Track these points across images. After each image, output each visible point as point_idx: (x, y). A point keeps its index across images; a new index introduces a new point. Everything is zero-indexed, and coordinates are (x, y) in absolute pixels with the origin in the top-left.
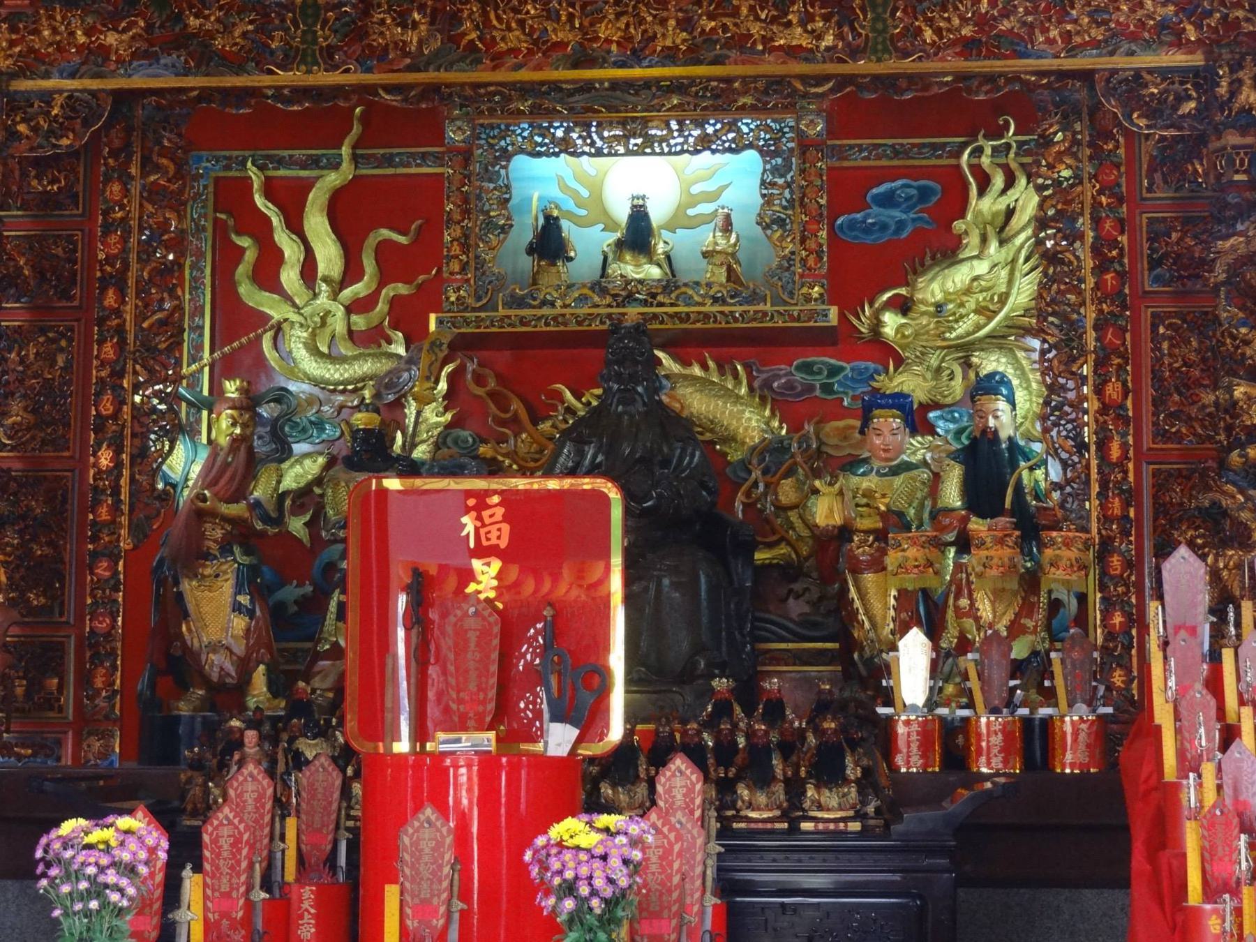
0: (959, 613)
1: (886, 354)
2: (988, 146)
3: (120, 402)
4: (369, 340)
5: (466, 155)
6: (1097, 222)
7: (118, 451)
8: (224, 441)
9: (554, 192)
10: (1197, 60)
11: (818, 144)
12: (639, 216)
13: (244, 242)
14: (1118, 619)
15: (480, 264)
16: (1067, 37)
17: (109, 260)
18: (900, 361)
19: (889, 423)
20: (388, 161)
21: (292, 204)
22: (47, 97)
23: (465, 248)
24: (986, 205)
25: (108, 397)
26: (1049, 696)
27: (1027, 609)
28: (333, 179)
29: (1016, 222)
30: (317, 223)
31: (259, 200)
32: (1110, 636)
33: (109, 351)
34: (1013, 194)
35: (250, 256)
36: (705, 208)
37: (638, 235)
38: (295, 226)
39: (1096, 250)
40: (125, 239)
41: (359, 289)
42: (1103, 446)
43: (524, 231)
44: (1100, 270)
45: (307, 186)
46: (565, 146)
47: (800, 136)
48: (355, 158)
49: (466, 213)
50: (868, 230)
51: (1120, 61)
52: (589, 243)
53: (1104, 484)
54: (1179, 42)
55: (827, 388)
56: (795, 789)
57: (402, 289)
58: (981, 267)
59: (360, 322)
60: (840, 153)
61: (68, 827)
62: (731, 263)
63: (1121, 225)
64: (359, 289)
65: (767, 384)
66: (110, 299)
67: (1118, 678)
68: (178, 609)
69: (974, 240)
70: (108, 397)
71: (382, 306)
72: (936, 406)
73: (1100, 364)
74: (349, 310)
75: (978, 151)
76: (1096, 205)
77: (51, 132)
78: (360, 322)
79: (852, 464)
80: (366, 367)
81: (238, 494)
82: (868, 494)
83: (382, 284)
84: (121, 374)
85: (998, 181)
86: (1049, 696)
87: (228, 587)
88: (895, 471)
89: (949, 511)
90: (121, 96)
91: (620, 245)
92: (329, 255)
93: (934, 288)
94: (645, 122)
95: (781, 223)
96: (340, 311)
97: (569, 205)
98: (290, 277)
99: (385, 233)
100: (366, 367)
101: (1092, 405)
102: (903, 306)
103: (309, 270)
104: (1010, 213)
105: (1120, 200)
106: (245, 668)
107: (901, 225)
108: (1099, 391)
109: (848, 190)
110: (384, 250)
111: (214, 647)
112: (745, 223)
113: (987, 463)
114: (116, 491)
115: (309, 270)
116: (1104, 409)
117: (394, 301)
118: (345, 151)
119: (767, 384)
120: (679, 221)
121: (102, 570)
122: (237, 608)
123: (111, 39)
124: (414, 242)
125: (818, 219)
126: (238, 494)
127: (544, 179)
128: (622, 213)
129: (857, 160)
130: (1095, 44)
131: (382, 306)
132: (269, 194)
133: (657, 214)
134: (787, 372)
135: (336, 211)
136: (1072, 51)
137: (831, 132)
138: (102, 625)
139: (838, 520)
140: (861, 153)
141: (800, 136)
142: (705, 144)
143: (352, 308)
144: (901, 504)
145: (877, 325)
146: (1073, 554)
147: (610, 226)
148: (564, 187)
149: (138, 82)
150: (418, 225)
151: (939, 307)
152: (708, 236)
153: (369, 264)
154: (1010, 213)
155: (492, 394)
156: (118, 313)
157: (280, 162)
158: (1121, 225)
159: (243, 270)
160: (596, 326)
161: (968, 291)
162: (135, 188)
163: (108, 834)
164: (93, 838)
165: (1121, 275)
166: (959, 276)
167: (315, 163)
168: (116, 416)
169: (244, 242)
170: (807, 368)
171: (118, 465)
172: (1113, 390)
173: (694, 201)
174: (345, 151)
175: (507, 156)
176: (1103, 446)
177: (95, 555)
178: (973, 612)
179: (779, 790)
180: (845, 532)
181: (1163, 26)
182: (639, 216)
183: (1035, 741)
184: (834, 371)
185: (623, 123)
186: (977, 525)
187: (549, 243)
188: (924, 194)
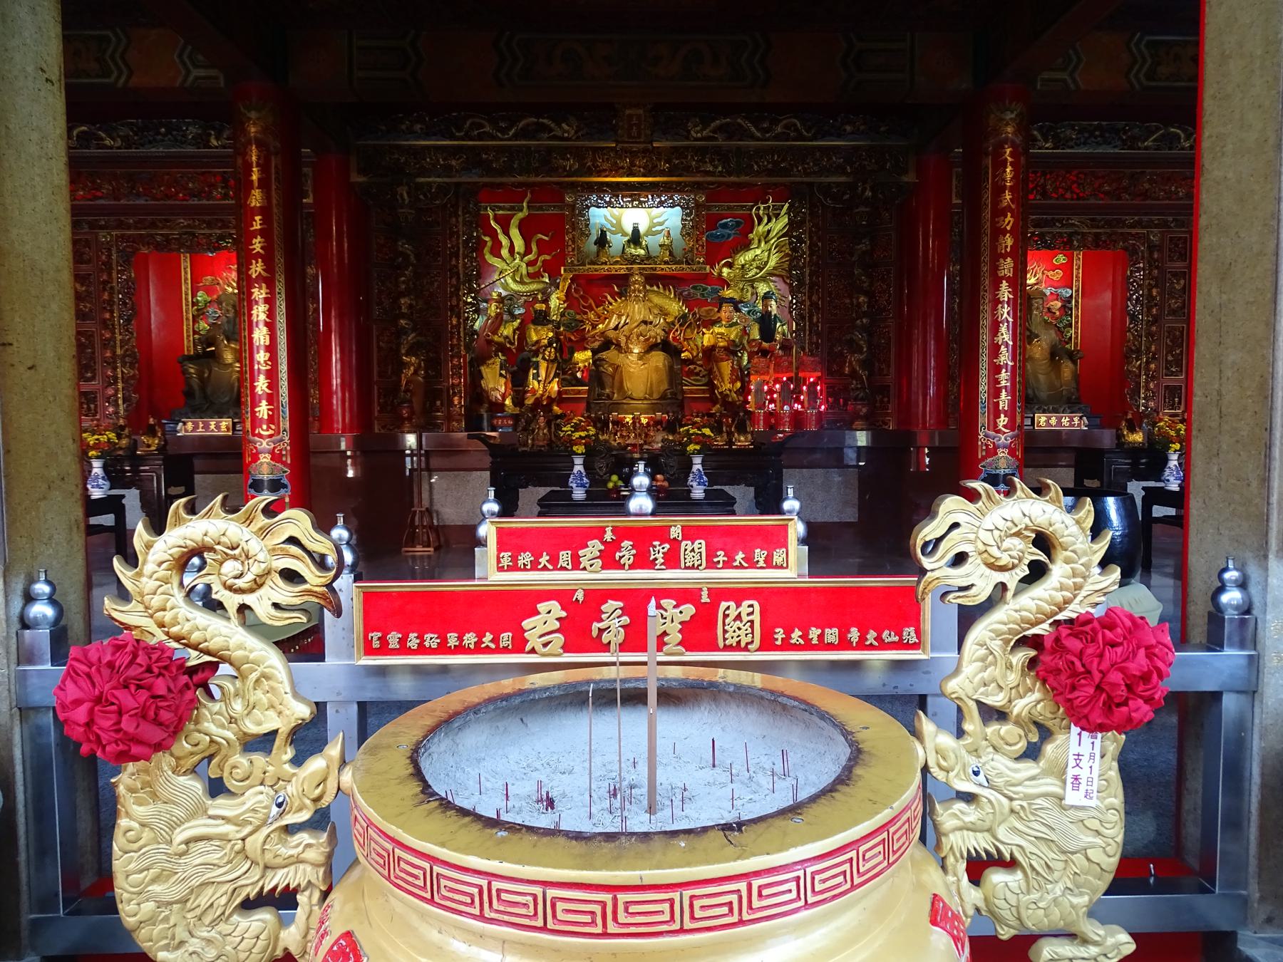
1: (724, 283)
2: (762, 207)
3: (459, 300)
4: (534, 276)
5: (573, 207)
6: (811, 238)
7: (459, 318)
9: (604, 222)
10: (849, 180)
12: (636, 230)
13: (487, 239)
15: (579, 248)
16: (805, 169)
17: (453, 247)
18: (729, 286)
19: (727, 310)
20: (540, 208)
21: (505, 224)
22: (430, 184)
23: (574, 242)
24: (761, 229)
28: (520, 215)
29: (771, 235)
30: (515, 232)
31: (492, 223)
34: (770, 225)
35: (489, 244)
36: (659, 228)
37: (635, 238)
38: (506, 233)
39: (810, 248)
41: (531, 257)
43: (594, 237)
44: (811, 255)
45: (511, 217)
46: (609, 204)
48: (528, 207)
49: (574, 229)
50: (717, 237)
51: (823, 179)
52: (617, 241)
54: (844, 173)
56: (730, 434)
57: (548, 257)
58: (758, 252)
59: (531, 270)
60: (709, 208)
64: (531, 257)
66: (454, 262)
69: (756, 241)
71: (539, 263)
74: (528, 265)
75: (758, 209)
76: (811, 232)
78: (531, 270)
80: (534, 287)
83: (539, 254)
84: (459, 290)
85: (765, 220)
88: (731, 326)
90: (458, 185)
92: (519, 244)
94: (639, 196)
95: (688, 234)
97: (609, 226)
98: (505, 252)
100: (534, 287)
101: (808, 303)
102: (730, 265)
104: (769, 231)
106: (504, 397)
107: (729, 235)
108: (810, 298)
109: (712, 222)
110: (539, 242)
112: (676, 234)
117: (544, 262)
118: (525, 204)
120: (650, 232)
122: (501, 375)
123: (454, 163)
124: (552, 238)
125: (702, 233)
127: (600, 216)
128: (629, 230)
129: (714, 211)
130: (815, 173)
131: (539, 263)
132: (496, 219)
133: (642, 230)
134: (688, 290)
135: (522, 227)
136: (807, 175)
137: (707, 200)
138: (456, 381)
139: (712, 342)
142: (661, 204)
143: (529, 264)
145: (720, 273)
147: (624, 234)
149: (464, 179)
150: (556, 235)
151: (743, 266)
152: (661, 239)
154: (769, 231)
155: (582, 297)
156: (456, 267)
157: (500, 208)
160: (622, 272)
162: (460, 219)
166: (749, 255)
167: (512, 209)
169: (487, 239)
171: (459, 323)
172: (814, 298)
174: (525, 204)
175: (588, 208)
177: (452, 357)
179: (725, 436)
182: (636, 230)
187: (602, 241)
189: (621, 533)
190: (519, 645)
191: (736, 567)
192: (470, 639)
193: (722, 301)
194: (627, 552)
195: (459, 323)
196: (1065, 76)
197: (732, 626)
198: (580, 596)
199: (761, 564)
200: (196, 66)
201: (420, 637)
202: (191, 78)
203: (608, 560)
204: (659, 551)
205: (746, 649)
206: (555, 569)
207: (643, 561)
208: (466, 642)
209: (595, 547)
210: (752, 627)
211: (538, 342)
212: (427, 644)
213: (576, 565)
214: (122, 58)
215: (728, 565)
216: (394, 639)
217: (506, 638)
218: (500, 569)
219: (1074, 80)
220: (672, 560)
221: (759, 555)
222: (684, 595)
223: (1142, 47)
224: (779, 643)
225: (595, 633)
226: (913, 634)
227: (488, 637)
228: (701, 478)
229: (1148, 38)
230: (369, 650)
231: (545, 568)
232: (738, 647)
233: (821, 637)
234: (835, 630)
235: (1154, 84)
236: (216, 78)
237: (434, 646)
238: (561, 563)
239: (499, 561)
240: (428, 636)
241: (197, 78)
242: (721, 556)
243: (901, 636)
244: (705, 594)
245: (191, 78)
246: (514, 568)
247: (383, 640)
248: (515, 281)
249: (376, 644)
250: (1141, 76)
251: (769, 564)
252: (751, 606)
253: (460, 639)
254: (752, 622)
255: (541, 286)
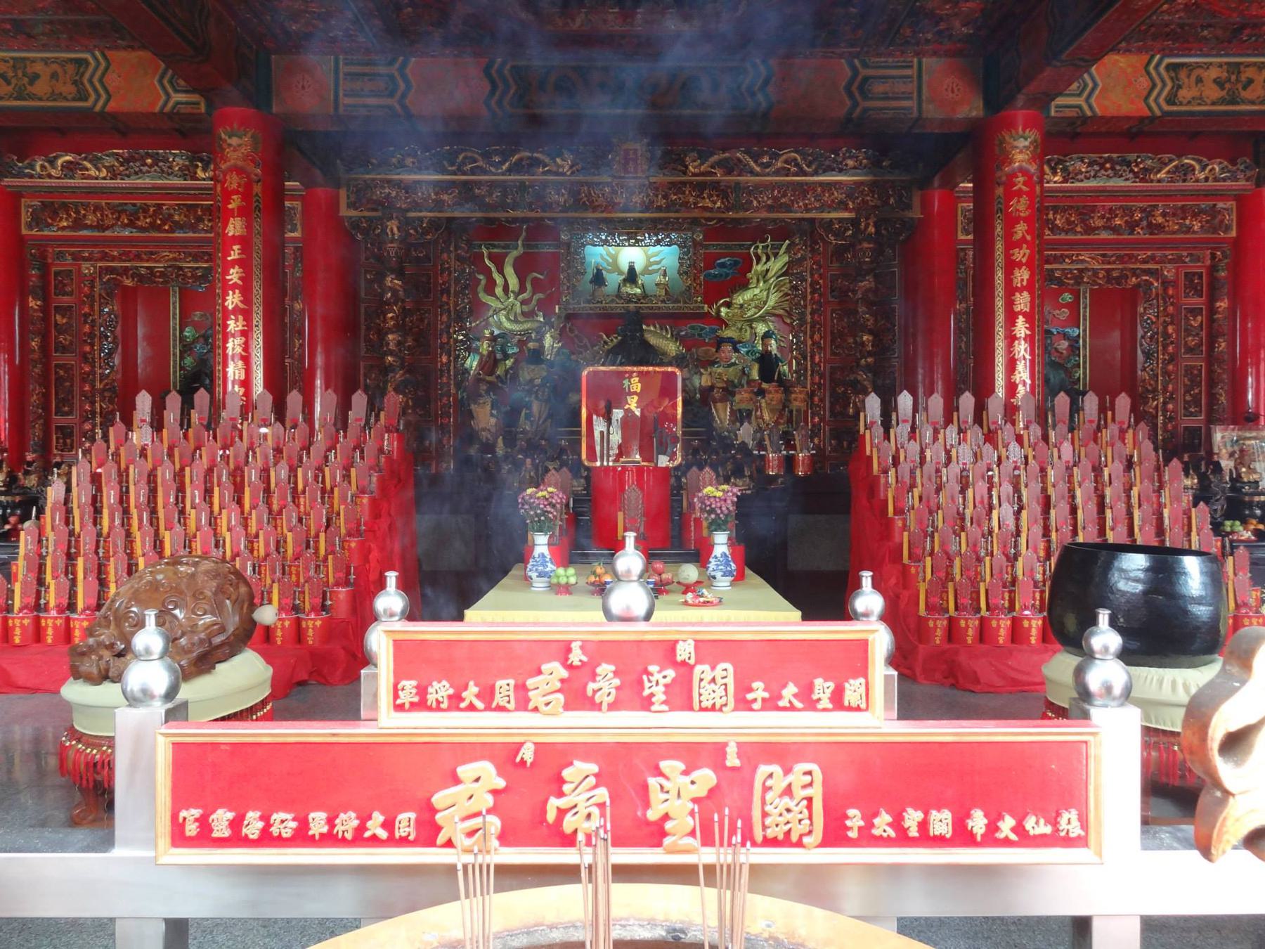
0: (757, 418)
1: (722, 322)
2: (761, 245)
3: (450, 337)
4: (529, 315)
5: (568, 245)
6: (812, 275)
7: (450, 356)
8: (485, 353)
9: (599, 260)
10: (852, 215)
11: (700, 244)
12: (632, 269)
13: (481, 277)
14: (817, 419)
16: (806, 205)
17: (444, 283)
18: (727, 325)
21: (499, 263)
22: (421, 219)
23: (569, 281)
24: (759, 268)
25: (445, 336)
26: (794, 448)
27: (781, 416)
28: (515, 254)
29: (771, 274)
30: (509, 270)
31: (487, 261)
32: (813, 425)
33: (445, 318)
35: (483, 282)
36: (655, 267)
37: (632, 276)
38: (501, 271)
40: (449, 274)
41: (525, 296)
42: (812, 357)
43: (589, 276)
44: (813, 293)
45: (506, 255)
46: (606, 243)
47: (694, 241)
49: (569, 267)
50: (715, 276)
51: (825, 215)
52: (613, 280)
53: (813, 371)
54: (846, 209)
55: (700, 335)
57: (541, 296)
58: (757, 291)
59: (526, 308)
60: (706, 247)
61: (529, 491)
62: (665, 286)
63: (821, 276)
65: (678, 334)
66: (445, 299)
67: (816, 441)
68: (471, 415)
69: (755, 280)
70: (445, 336)
71: (534, 302)
72: (740, 342)
73: (812, 327)
75: (757, 248)
76: (812, 269)
77: (423, 234)
78: (526, 308)
79: (713, 363)
81: (491, 373)
82: (720, 374)
83: (534, 294)
85: (764, 259)
86: (794, 448)
87: (488, 407)
88: (730, 366)
89: (754, 381)
90: (450, 220)
91: (624, 280)
92: (513, 282)
93: (740, 299)
94: (636, 234)
95: (686, 273)
96: (518, 304)
97: (605, 265)
98: (499, 290)
99: (535, 275)
101: (809, 342)
102: (728, 305)
103: (506, 288)
104: (767, 271)
105: (820, 267)
107: (727, 275)
108: (812, 337)
109: (710, 261)
110: (535, 281)
111: (484, 429)
113: (767, 363)
114: (449, 370)
115: (506, 288)
116: (813, 344)
117: (539, 301)
118: (520, 243)
119: (678, 334)
120: (646, 271)
121: (445, 400)
122: (492, 415)
123: (445, 197)
125: (700, 272)
126: (491, 373)
127: (597, 254)
128: (625, 268)
130: (816, 208)
131: (534, 302)
132: (491, 257)
133: (638, 268)
136: (808, 210)
137: (706, 238)
140: (715, 247)
141: (694, 241)
142: (658, 242)
143: (523, 303)
144: (732, 378)
145: (718, 311)
146: (802, 396)
147: (621, 273)
148: (602, 258)
149: (457, 214)
151: (741, 306)
152: (658, 278)
153: (529, 286)
154: (767, 271)
157: (494, 246)
158: (821, 276)
159: (480, 288)
161: (752, 300)
162: (453, 256)
163: (544, 493)
164: (540, 494)
165: (820, 295)
166: (748, 295)
168: (448, 343)
169: (481, 277)
170: (693, 328)
171: (450, 361)
172: (817, 337)
173: (652, 264)
174: (520, 243)
175: (584, 246)
176: (812, 357)
178: (762, 417)
180: (712, 388)
181: (841, 202)
182: (632, 269)
183: (790, 462)
184: (702, 329)
185: (628, 234)
186: (765, 385)
187: (598, 279)
188: (736, 263)
189: (600, 651)
190: (428, 833)
191: (784, 709)
192: (347, 823)
193: (719, 342)
194: (606, 682)
195: (450, 361)
196: (1079, 101)
197: (776, 804)
198: (527, 754)
199: (825, 703)
200: (176, 91)
201: (266, 818)
202: (170, 104)
203: (577, 696)
204: (659, 679)
205: (799, 844)
206: (488, 708)
207: (633, 696)
208: (339, 829)
209: (555, 671)
210: (809, 807)
211: (531, 381)
212: (275, 831)
213: (523, 703)
214: (101, 81)
215: (771, 704)
216: (221, 819)
217: (406, 822)
218: (399, 708)
219: (1090, 107)
220: (682, 696)
221: (823, 689)
222: (694, 754)
223: (1162, 69)
224: (853, 834)
225: (551, 816)
226: (1075, 823)
227: (378, 818)
228: (727, 564)
229: (1168, 60)
230: (179, 838)
231: (472, 708)
232: (785, 841)
233: (923, 825)
234: (946, 815)
235: (1175, 108)
236: (198, 104)
237: (287, 834)
238: (499, 699)
239: (396, 696)
240: (277, 817)
241: (178, 103)
242: (759, 691)
243: (1055, 824)
244: (732, 750)
245: (170, 104)
246: (421, 705)
247: (204, 822)
248: (508, 319)
249: (192, 829)
250: (1161, 100)
251: (838, 702)
252: (809, 773)
253: (331, 822)
254: (810, 800)
255: (535, 325)
